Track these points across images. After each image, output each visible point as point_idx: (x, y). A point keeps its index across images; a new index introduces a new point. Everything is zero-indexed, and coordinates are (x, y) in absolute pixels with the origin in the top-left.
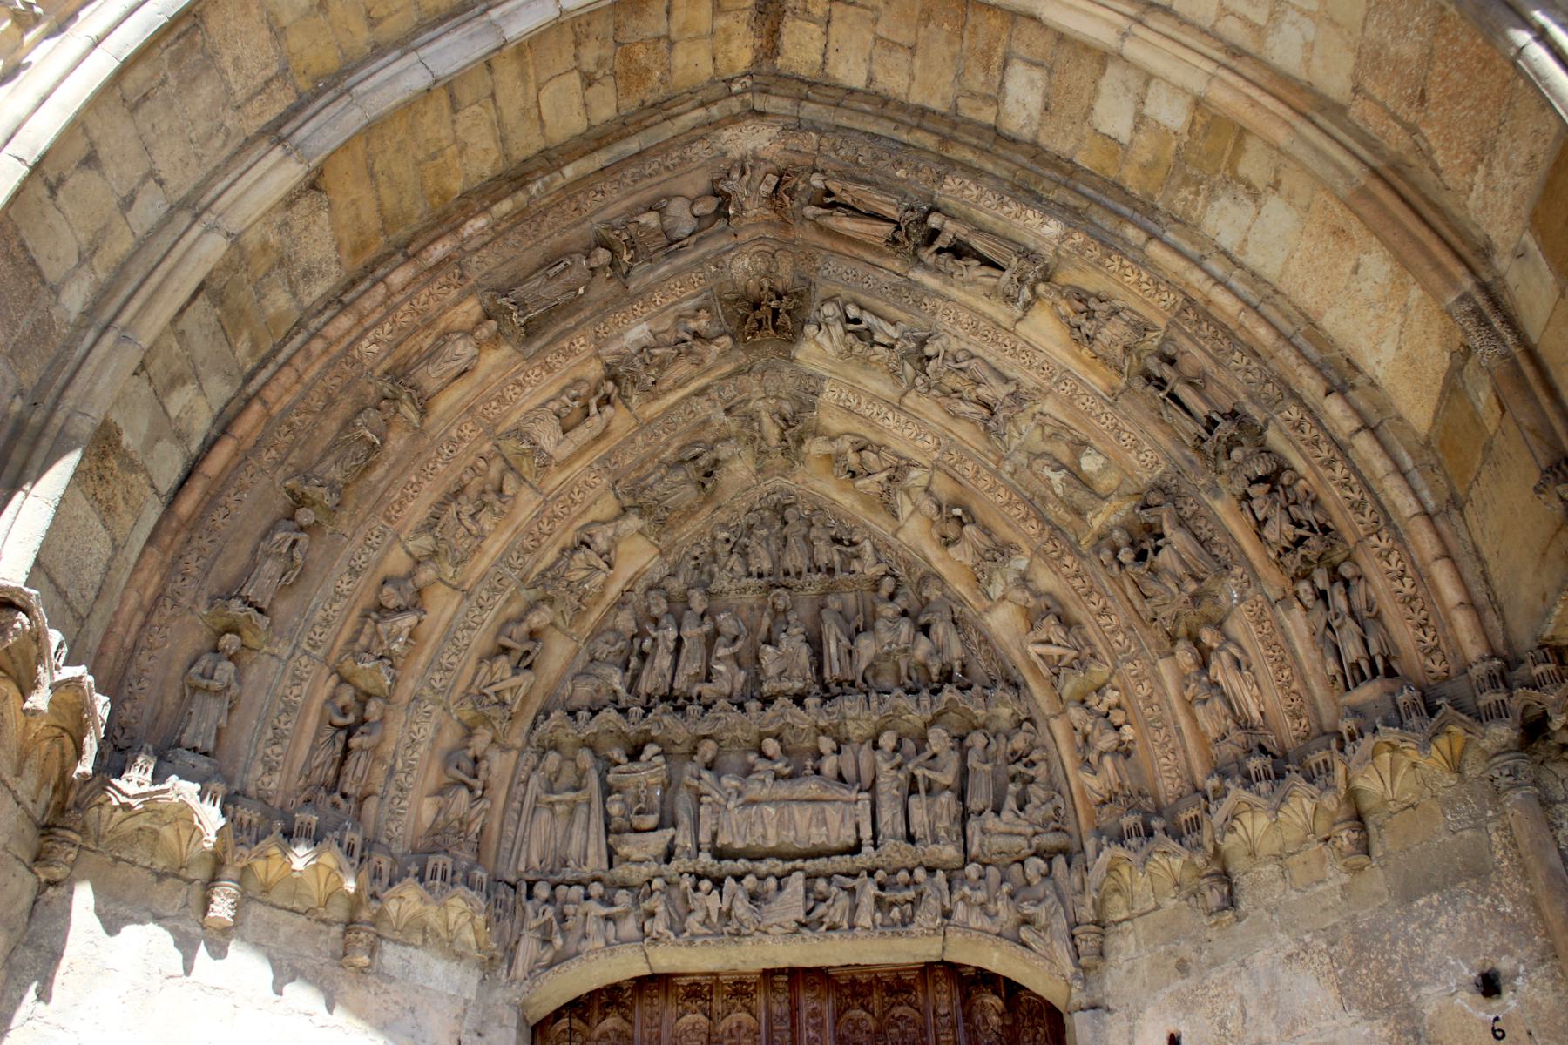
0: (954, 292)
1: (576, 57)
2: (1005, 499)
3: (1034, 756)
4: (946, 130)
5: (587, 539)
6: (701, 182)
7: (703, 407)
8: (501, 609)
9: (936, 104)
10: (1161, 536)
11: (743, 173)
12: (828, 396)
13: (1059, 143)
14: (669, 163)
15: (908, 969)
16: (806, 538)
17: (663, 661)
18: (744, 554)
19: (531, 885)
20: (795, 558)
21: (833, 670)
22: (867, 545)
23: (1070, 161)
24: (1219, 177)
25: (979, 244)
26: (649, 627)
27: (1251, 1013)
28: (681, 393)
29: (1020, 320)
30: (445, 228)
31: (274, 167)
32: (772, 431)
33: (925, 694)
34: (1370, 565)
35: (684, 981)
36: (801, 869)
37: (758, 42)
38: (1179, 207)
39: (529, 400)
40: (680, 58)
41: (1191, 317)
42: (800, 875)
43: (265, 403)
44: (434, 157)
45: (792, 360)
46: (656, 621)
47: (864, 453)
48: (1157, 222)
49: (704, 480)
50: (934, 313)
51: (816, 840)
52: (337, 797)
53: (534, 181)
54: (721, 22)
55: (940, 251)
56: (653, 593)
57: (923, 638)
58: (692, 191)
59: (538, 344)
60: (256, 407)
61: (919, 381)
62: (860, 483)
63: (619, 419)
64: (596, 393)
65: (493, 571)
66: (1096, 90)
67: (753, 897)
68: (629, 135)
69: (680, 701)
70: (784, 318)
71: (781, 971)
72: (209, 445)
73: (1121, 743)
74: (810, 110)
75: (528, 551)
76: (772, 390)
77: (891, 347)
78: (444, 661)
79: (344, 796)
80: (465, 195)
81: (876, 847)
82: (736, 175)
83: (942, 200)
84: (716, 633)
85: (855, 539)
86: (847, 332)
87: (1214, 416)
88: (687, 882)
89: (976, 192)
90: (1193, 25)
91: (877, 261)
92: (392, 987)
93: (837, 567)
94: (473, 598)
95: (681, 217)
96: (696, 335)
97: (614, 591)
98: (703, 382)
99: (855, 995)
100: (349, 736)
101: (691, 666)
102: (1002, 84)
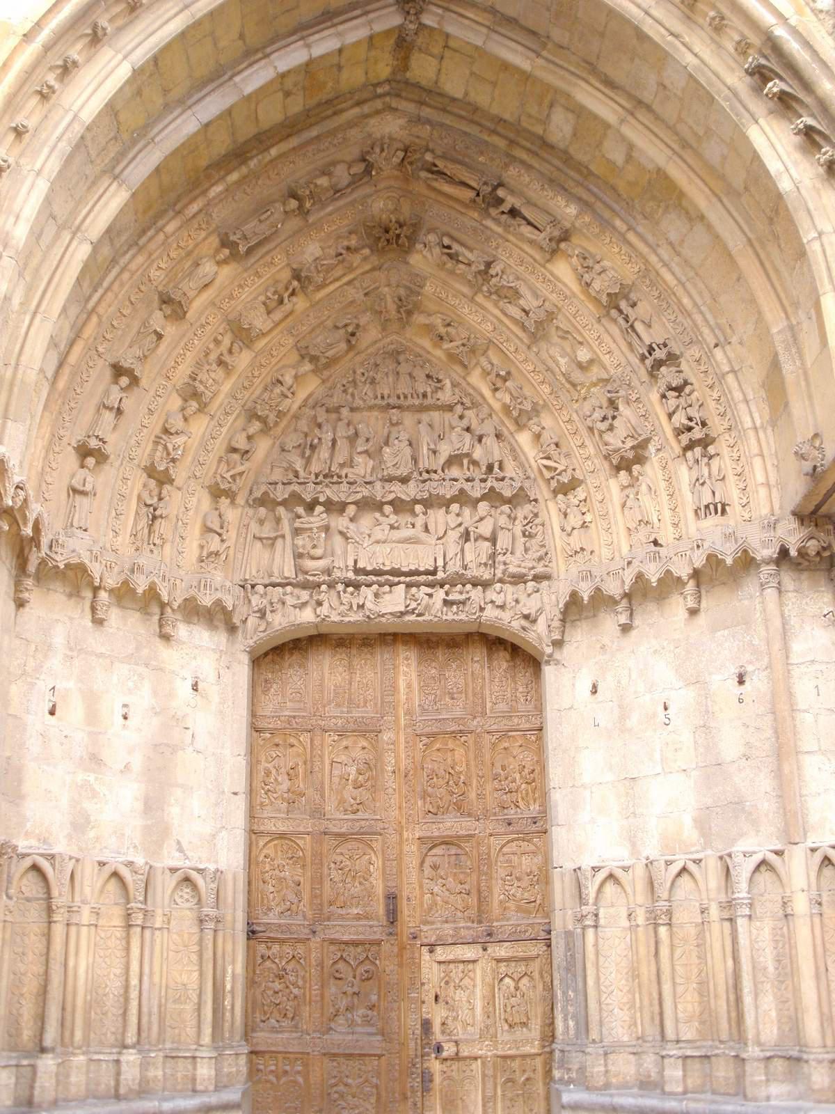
0: (511, 238)
1: (282, 84)
2: (531, 368)
3: (537, 521)
4: (511, 135)
5: (280, 378)
6: (355, 152)
7: (351, 293)
8: (232, 424)
9: (507, 116)
10: (617, 409)
11: (382, 150)
12: (428, 289)
13: (580, 156)
14: (335, 142)
15: (458, 635)
16: (410, 374)
17: (324, 453)
18: (373, 381)
19: (253, 587)
20: (403, 387)
21: (424, 463)
22: (447, 383)
23: (587, 168)
24: (671, 202)
25: (526, 212)
26: (317, 431)
27: (634, 677)
28: (337, 284)
29: (548, 261)
30: (197, 192)
31: (113, 196)
32: (392, 307)
33: (477, 482)
34: (725, 452)
35: (335, 637)
36: (403, 583)
37: (395, 63)
38: (648, 210)
39: (246, 295)
40: (345, 75)
41: (648, 282)
42: (403, 586)
43: (99, 317)
44: (193, 151)
45: (407, 263)
46: (320, 426)
47: (449, 329)
48: (634, 218)
49: (351, 338)
50: (497, 248)
51: (413, 568)
52: (152, 546)
53: (251, 158)
54: (373, 53)
55: (503, 213)
56: (318, 409)
57: (478, 446)
58: (349, 158)
59: (252, 260)
60: (94, 319)
61: (485, 288)
62: (446, 346)
63: (300, 303)
64: (287, 289)
65: (227, 401)
66: (605, 134)
67: (376, 595)
68: (311, 125)
69: (335, 479)
70: (403, 240)
71: (390, 634)
72: (72, 344)
73: (585, 522)
74: (426, 112)
75: (245, 388)
76: (393, 281)
77: (469, 265)
78: (201, 459)
79: (154, 545)
80: (207, 168)
81: (444, 571)
82: (377, 150)
83: (506, 180)
84: (356, 434)
85: (441, 377)
86: (443, 254)
87: (654, 345)
88: (340, 587)
89: (527, 179)
90: (663, 121)
91: (463, 210)
92: (184, 646)
93: (429, 395)
94: (216, 418)
95: (342, 175)
96: (348, 248)
97: (295, 406)
98: (351, 276)
99: (430, 648)
100: (155, 510)
101: (340, 457)
102: (548, 115)
